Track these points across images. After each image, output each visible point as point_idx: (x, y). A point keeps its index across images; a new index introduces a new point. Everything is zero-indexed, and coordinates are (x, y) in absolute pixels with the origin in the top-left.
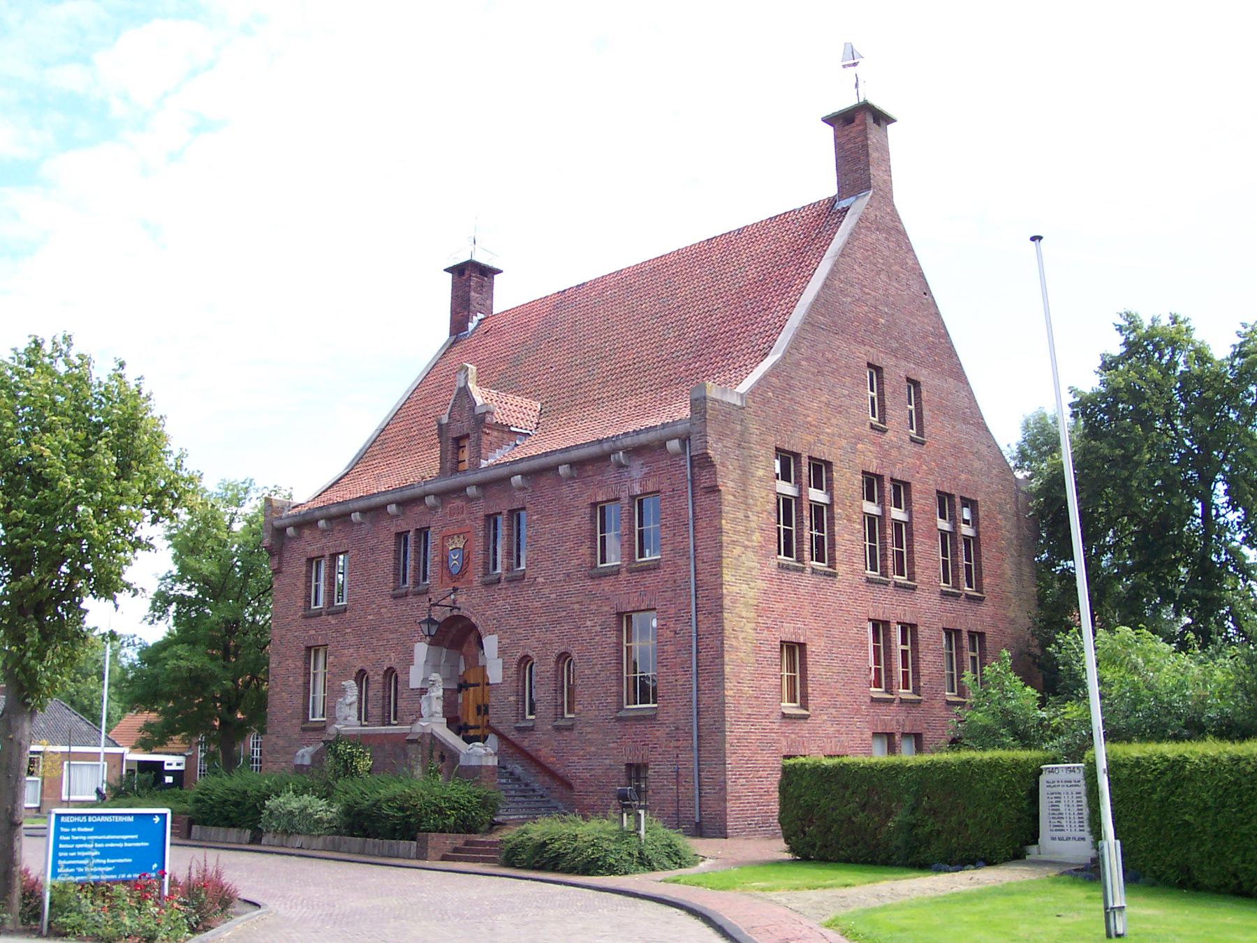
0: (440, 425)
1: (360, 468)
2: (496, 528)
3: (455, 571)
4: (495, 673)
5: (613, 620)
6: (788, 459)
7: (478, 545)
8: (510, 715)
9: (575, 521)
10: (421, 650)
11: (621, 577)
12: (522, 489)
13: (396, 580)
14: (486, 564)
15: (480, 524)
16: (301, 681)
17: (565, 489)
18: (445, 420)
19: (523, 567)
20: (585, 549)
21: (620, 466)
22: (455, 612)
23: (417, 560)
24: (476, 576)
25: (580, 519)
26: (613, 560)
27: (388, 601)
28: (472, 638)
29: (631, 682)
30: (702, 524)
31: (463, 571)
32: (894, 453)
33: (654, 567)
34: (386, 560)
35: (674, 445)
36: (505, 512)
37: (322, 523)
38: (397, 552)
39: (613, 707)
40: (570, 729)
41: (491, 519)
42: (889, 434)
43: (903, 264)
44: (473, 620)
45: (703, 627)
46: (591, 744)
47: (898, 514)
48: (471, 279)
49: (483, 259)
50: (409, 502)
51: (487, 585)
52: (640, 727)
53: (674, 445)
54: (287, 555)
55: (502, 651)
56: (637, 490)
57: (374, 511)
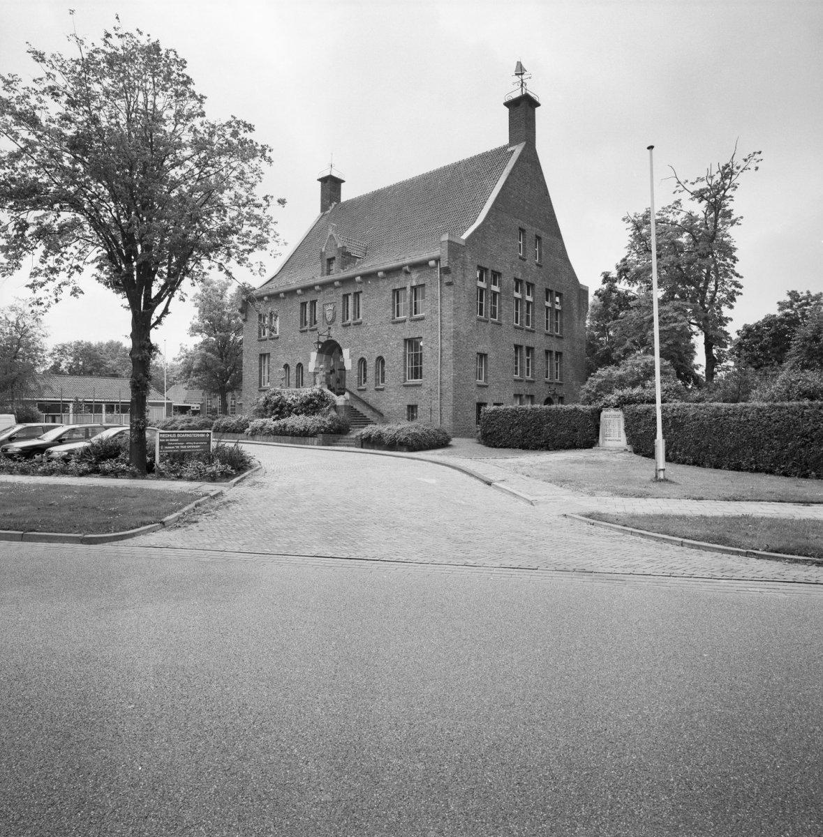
0: (321, 253)
1: (281, 274)
2: (348, 301)
3: (329, 320)
4: (348, 365)
5: (402, 342)
6: (483, 270)
7: (340, 309)
8: (355, 385)
9: (386, 297)
10: (314, 355)
11: (406, 323)
12: (360, 283)
13: (301, 324)
14: (343, 316)
15: (341, 298)
16: (258, 369)
17: (381, 283)
18: (323, 250)
19: (361, 318)
20: (390, 311)
21: (407, 273)
22: (330, 339)
23: (311, 315)
24: (339, 322)
25: (388, 296)
26: (402, 317)
27: (298, 333)
28: (337, 350)
29: (410, 370)
30: (444, 299)
31: (333, 321)
32: (528, 270)
33: (422, 319)
34: (296, 315)
35: (432, 263)
36: (352, 294)
37: (266, 298)
38: (302, 311)
39: (402, 381)
40: (382, 390)
41: (346, 296)
42: (527, 261)
43: (538, 180)
44: (338, 342)
45: (444, 345)
46: (392, 396)
47: (529, 298)
48: (331, 185)
49: (335, 174)
50: (307, 289)
51: (344, 326)
52: (414, 389)
53: (432, 263)
54: (249, 312)
55: (351, 356)
56: (414, 284)
57: (291, 293)
